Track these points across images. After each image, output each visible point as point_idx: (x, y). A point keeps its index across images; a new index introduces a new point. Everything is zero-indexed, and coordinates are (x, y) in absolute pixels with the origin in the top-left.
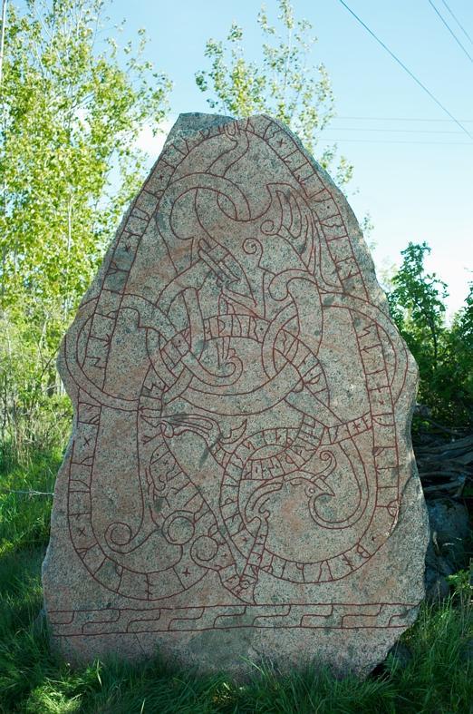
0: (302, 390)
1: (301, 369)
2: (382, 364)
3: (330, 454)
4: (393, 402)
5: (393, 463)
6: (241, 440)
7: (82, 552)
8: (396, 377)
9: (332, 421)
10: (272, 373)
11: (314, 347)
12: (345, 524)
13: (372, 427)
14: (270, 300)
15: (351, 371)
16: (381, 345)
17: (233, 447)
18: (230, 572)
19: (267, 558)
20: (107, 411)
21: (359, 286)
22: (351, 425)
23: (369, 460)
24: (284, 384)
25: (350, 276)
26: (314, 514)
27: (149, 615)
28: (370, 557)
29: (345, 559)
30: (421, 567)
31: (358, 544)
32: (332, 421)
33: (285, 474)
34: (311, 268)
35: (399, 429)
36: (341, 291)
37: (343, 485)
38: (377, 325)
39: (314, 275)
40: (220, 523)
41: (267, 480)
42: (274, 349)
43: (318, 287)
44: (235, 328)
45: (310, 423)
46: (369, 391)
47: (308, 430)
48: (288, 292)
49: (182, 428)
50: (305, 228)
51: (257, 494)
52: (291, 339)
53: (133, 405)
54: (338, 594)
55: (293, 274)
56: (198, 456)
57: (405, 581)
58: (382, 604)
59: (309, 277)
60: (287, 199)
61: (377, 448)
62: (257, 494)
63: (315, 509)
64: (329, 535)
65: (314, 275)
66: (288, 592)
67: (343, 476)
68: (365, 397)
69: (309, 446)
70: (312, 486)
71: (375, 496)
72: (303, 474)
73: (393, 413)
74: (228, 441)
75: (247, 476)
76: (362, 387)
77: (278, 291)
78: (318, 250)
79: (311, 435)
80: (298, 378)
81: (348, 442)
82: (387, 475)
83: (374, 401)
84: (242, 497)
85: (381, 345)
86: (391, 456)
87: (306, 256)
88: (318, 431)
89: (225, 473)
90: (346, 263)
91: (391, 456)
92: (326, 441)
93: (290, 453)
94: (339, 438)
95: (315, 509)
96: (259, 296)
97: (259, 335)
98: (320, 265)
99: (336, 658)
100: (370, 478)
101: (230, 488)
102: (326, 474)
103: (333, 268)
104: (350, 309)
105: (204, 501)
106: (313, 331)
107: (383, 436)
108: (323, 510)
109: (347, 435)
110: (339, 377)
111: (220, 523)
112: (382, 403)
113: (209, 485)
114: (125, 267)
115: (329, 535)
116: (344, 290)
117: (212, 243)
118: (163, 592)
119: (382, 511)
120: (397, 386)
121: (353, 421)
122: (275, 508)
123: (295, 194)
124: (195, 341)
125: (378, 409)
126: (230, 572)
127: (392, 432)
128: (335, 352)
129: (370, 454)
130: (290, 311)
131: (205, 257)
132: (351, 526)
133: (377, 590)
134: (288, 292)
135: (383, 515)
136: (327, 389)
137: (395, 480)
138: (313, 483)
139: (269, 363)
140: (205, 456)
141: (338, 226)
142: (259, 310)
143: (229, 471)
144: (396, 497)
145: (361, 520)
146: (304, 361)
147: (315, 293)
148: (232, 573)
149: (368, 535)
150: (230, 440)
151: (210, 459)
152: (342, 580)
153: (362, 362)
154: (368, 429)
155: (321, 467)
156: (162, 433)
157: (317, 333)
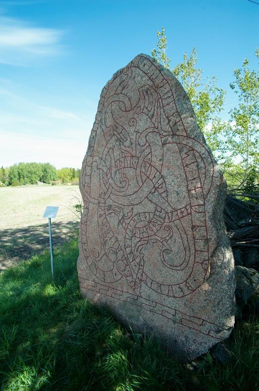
0: (155, 192)
1: (154, 181)
2: (197, 173)
3: (169, 228)
4: (204, 197)
5: (204, 237)
6: (131, 218)
7: (87, 257)
8: (206, 181)
9: (169, 209)
10: (141, 184)
11: (159, 168)
12: (179, 268)
13: (191, 213)
14: (139, 146)
15: (178, 180)
16: (196, 162)
17: (129, 221)
18: (130, 279)
19: (144, 277)
20: (91, 204)
21: (181, 128)
22: (179, 211)
23: (190, 233)
24: (146, 190)
25: (176, 123)
26: (163, 260)
27: (105, 288)
28: (194, 291)
29: (180, 288)
30: (228, 306)
31: (186, 281)
32: (169, 209)
33: (149, 236)
34: (156, 125)
35: (207, 215)
36: (171, 134)
37: (176, 245)
38: (193, 150)
39: (157, 128)
40: (126, 256)
41: (142, 238)
42: (141, 172)
43: (160, 134)
44: (126, 164)
45: (159, 210)
46: (189, 191)
47: (158, 214)
48: (147, 141)
49: (111, 211)
50: (154, 104)
51: (138, 245)
52: (148, 165)
53: (96, 202)
54: (177, 305)
55: (149, 130)
56: (116, 224)
57: (217, 312)
58: (203, 320)
59: (156, 130)
60: (147, 92)
61: (195, 226)
62: (138, 245)
63: (163, 257)
64: (171, 273)
65: (157, 128)
66: (155, 296)
67: (176, 241)
68: (187, 195)
69: (159, 223)
70: (161, 244)
71: (193, 256)
72: (157, 238)
73: (204, 204)
74: (126, 218)
75: (134, 235)
76: (185, 189)
77: (142, 141)
78: (159, 114)
79: (160, 217)
80: (153, 186)
81: (178, 221)
82: (201, 244)
83: (192, 197)
84: (133, 245)
85: (196, 162)
86: (203, 232)
87: (154, 120)
88: (163, 215)
89: (126, 233)
90: (173, 116)
91: (203, 232)
92: (167, 220)
93: (151, 225)
94: (173, 219)
95: (163, 257)
96: (134, 145)
97: (134, 165)
98: (160, 122)
99: (180, 339)
100: (190, 244)
101: (128, 240)
102: (167, 238)
103: (167, 121)
104: (177, 143)
105: (119, 245)
106: (158, 159)
107: (197, 219)
108: (167, 258)
109: (177, 218)
110: (173, 184)
111: (126, 256)
112: (197, 198)
113: (120, 237)
114: (93, 145)
115: (171, 273)
116: (173, 133)
117: (118, 126)
118: (109, 280)
119: (198, 265)
120: (206, 187)
121: (180, 209)
122: (146, 253)
123: (150, 89)
124: (113, 172)
125: (195, 202)
126: (130, 279)
127: (203, 217)
128: (171, 169)
129: (191, 229)
130: (148, 151)
131: (115, 133)
132: (182, 270)
133: (200, 311)
134: (147, 141)
135: (199, 268)
136: (166, 191)
137: (206, 248)
138: (162, 242)
139: (139, 179)
140: (119, 224)
141: (170, 97)
142: (134, 153)
143: (128, 232)
144: (207, 258)
145: (187, 268)
146: (154, 176)
147: (158, 138)
148: (131, 279)
149: (192, 278)
150: (128, 218)
151: (121, 226)
152: (179, 299)
153: (185, 174)
154: (188, 214)
155: (165, 234)
156: (105, 213)
157: (160, 160)
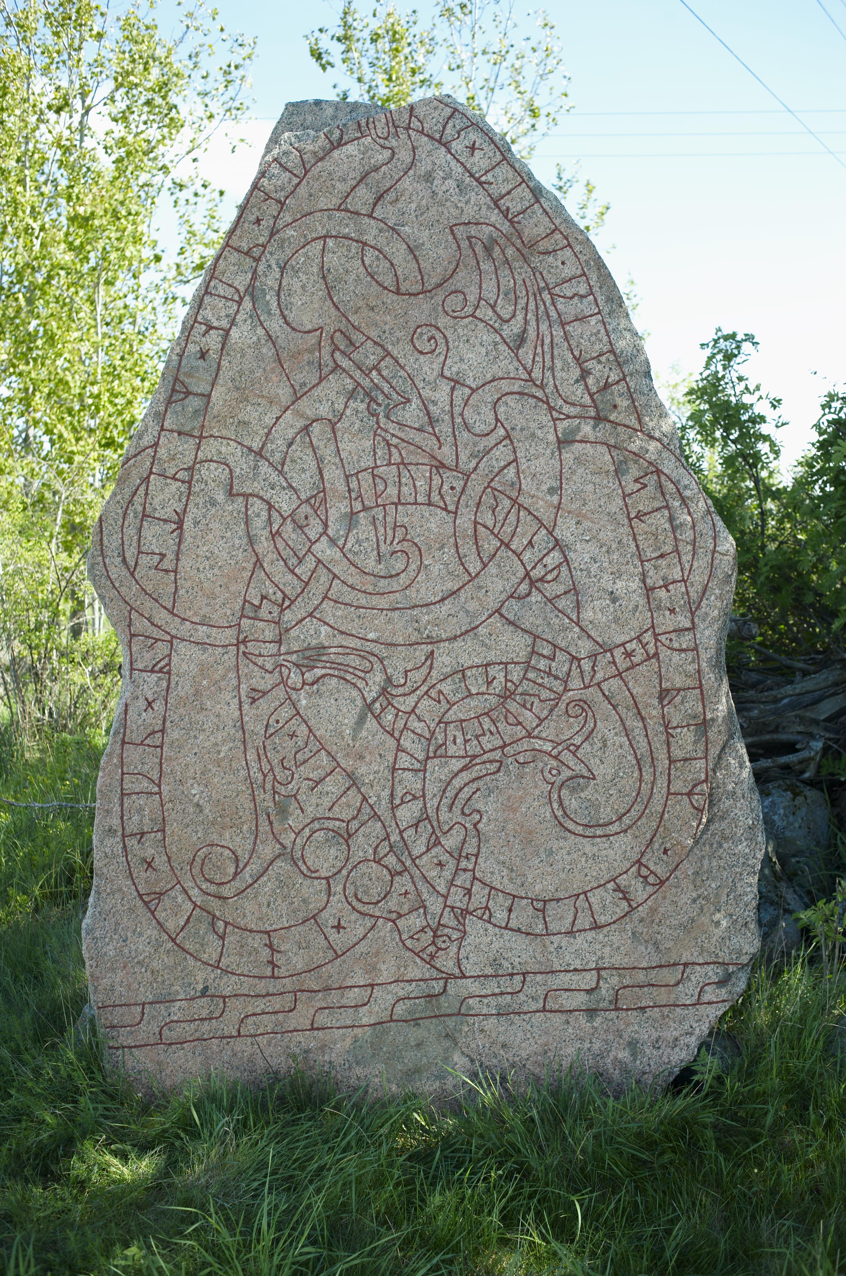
0: (528, 595)
1: (527, 556)
2: (670, 541)
3: (584, 705)
4: (693, 609)
6: (424, 689)
7: (151, 900)
8: (696, 564)
9: (584, 648)
10: (474, 566)
11: (546, 516)
13: (656, 655)
14: (465, 434)
16: (667, 507)
17: (411, 701)
18: (416, 921)
19: (480, 894)
21: (623, 403)
23: (654, 713)
24: (496, 584)
25: (607, 386)
26: (559, 813)
27: (277, 1003)
28: (662, 883)
29: (618, 889)
30: (750, 896)
31: (638, 861)
32: (584, 648)
33: (505, 745)
34: (537, 374)
35: (705, 656)
36: (593, 414)
37: (609, 759)
38: (658, 472)
39: (542, 387)
41: (475, 757)
42: (476, 523)
43: (551, 409)
44: (405, 489)
45: (545, 652)
46: (649, 590)
47: (542, 664)
48: (497, 420)
49: (319, 672)
50: (522, 302)
51: (457, 783)
52: (507, 503)
53: (229, 636)
54: (607, 950)
55: (505, 386)
56: (350, 720)
57: (724, 923)
58: (686, 965)
59: (534, 390)
60: (488, 250)
61: (668, 691)
62: (457, 783)
63: (561, 804)
64: (588, 849)
65: (542, 387)
66: (520, 951)
67: (609, 743)
68: (642, 601)
69: (545, 694)
70: (554, 763)
72: (538, 744)
73: (693, 628)
74: (400, 691)
75: (437, 752)
76: (635, 584)
77: (481, 419)
78: (547, 341)
79: (549, 674)
80: (521, 573)
81: (615, 683)
82: (686, 739)
83: (659, 608)
84: (432, 789)
85: (667, 507)
86: (692, 704)
87: (526, 353)
88: (561, 666)
90: (600, 362)
91: (692, 704)
92: (575, 683)
93: (512, 706)
94: (599, 676)
95: (561, 804)
96: (444, 428)
97: (448, 499)
98: (552, 369)
100: (656, 745)
101: (408, 775)
102: (578, 740)
103: (577, 373)
104: (608, 446)
105: (365, 799)
106: (545, 488)
107: (677, 668)
108: (574, 804)
110: (594, 568)
112: (672, 611)
113: (371, 770)
114: (203, 388)
115: (588, 849)
116: (598, 412)
117: (357, 337)
118: (299, 962)
120: (698, 579)
121: (623, 644)
122: (490, 807)
123: (502, 241)
124: (333, 515)
126: (416, 921)
127: (693, 661)
128: (586, 524)
129: (655, 702)
130: (502, 454)
131: (345, 363)
132: (625, 831)
134: (497, 420)
135: (682, 808)
136: (574, 590)
137: (701, 747)
138: (556, 758)
139: (469, 549)
140: (361, 721)
141: (582, 297)
142: (446, 453)
143: (406, 743)
144: (703, 777)
145: (644, 819)
146: (530, 542)
147: (545, 419)
149: (656, 846)
151: (371, 723)
152: (613, 927)
153: (635, 539)
154: (649, 658)
155: (570, 729)
156: (284, 682)
